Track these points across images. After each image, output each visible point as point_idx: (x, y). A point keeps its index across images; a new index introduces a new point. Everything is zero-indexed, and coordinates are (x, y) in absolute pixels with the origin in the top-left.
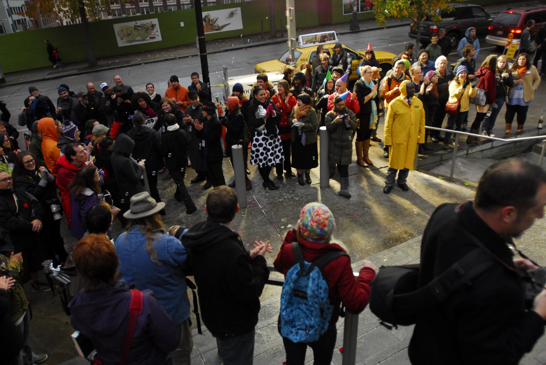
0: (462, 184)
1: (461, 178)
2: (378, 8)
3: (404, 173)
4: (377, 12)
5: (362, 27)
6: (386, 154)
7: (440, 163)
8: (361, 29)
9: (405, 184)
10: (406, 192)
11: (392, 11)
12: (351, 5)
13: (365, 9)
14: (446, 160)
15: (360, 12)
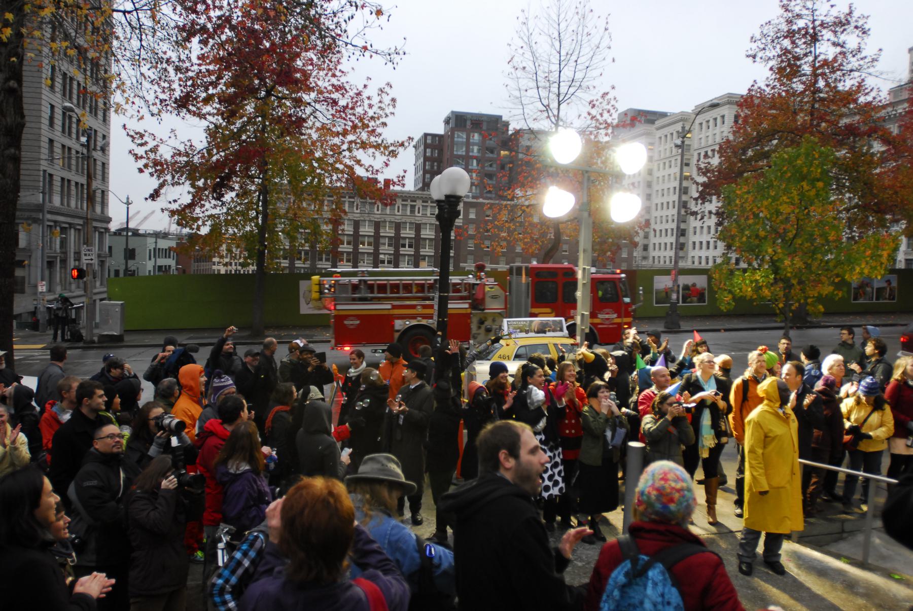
0: (888, 574)
1: (888, 565)
2: (721, 283)
3: (774, 541)
4: (719, 288)
5: (684, 326)
6: (739, 511)
7: (841, 535)
8: (683, 328)
9: (778, 562)
10: (780, 577)
11: (744, 287)
12: (667, 293)
13: (689, 300)
14: (852, 533)
15: (681, 304)
